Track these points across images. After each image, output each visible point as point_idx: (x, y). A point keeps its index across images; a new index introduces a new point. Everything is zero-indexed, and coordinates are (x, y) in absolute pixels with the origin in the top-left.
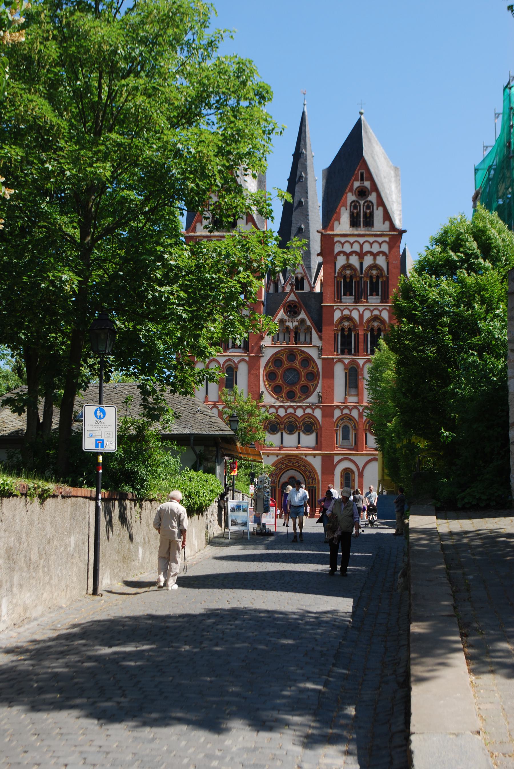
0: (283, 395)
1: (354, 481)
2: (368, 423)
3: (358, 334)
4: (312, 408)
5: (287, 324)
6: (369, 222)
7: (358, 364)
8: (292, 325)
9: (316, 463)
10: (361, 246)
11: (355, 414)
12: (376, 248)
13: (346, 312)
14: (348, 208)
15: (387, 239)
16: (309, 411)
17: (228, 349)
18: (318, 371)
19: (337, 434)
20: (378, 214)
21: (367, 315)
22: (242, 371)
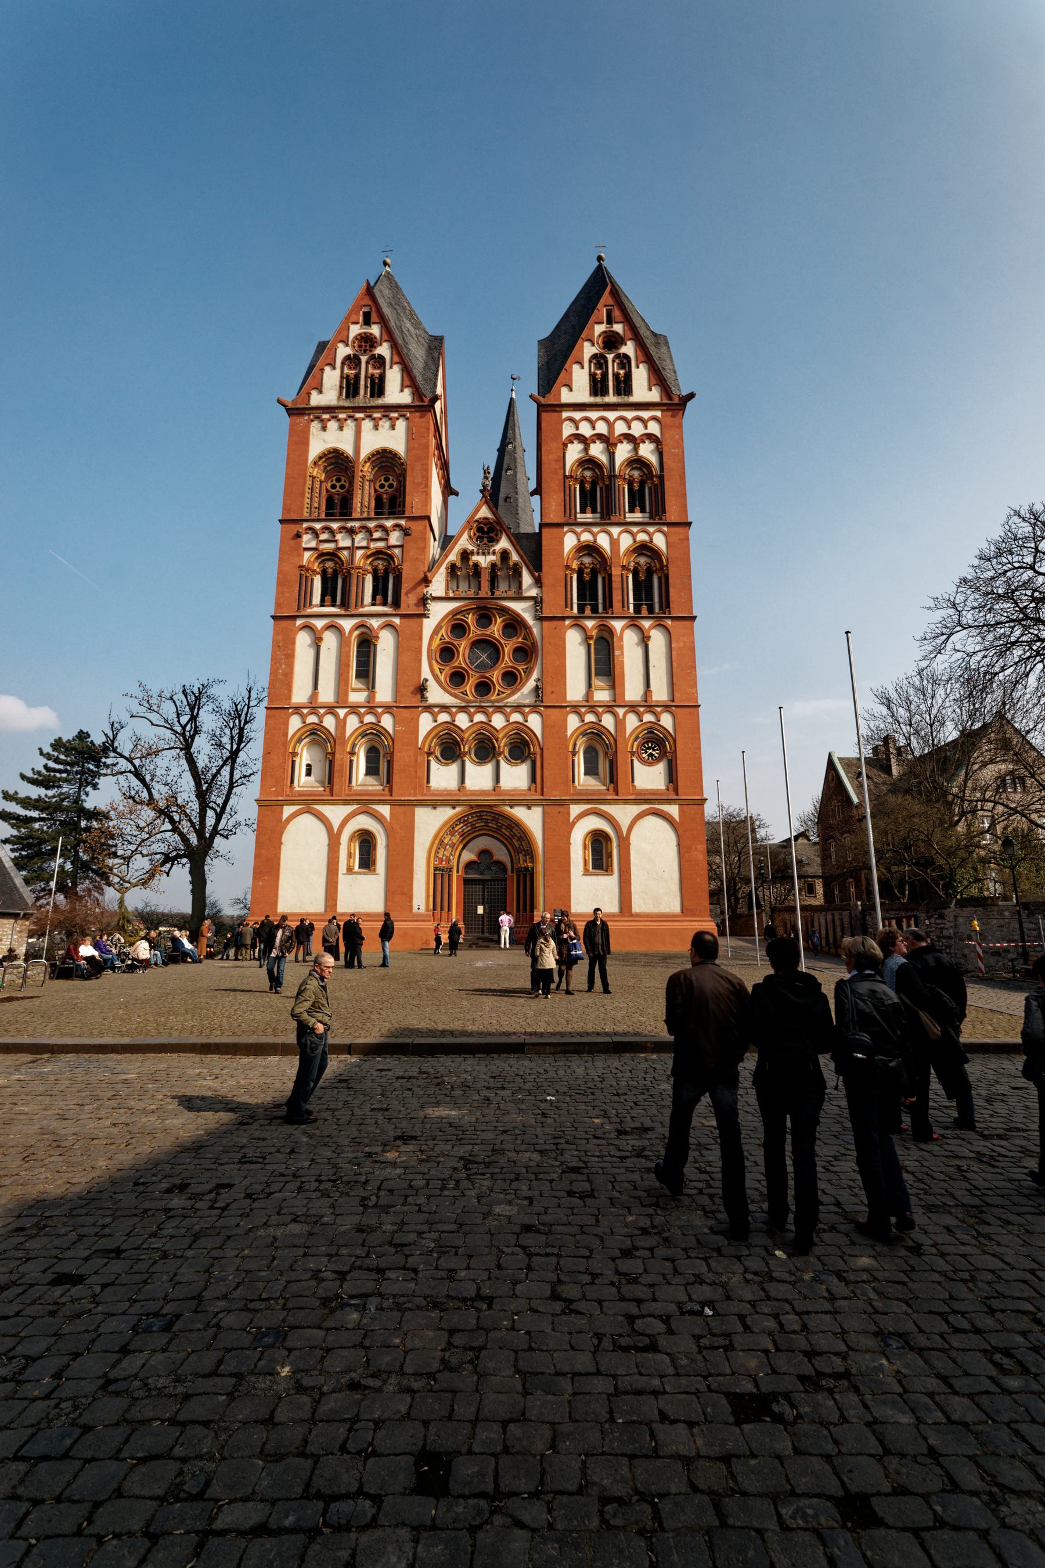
0: (468, 688)
1: (610, 855)
2: (635, 740)
3: (610, 576)
4: (522, 713)
5: (475, 558)
6: (624, 386)
7: (610, 631)
8: (484, 561)
9: (532, 819)
10: (611, 425)
11: (608, 721)
12: (637, 429)
13: (586, 537)
14: (586, 365)
15: (658, 414)
16: (516, 717)
17: (362, 606)
18: (534, 644)
19: (573, 761)
20: (640, 375)
21: (626, 542)
22: (386, 645)
